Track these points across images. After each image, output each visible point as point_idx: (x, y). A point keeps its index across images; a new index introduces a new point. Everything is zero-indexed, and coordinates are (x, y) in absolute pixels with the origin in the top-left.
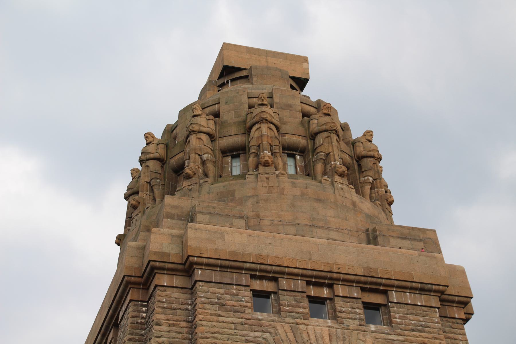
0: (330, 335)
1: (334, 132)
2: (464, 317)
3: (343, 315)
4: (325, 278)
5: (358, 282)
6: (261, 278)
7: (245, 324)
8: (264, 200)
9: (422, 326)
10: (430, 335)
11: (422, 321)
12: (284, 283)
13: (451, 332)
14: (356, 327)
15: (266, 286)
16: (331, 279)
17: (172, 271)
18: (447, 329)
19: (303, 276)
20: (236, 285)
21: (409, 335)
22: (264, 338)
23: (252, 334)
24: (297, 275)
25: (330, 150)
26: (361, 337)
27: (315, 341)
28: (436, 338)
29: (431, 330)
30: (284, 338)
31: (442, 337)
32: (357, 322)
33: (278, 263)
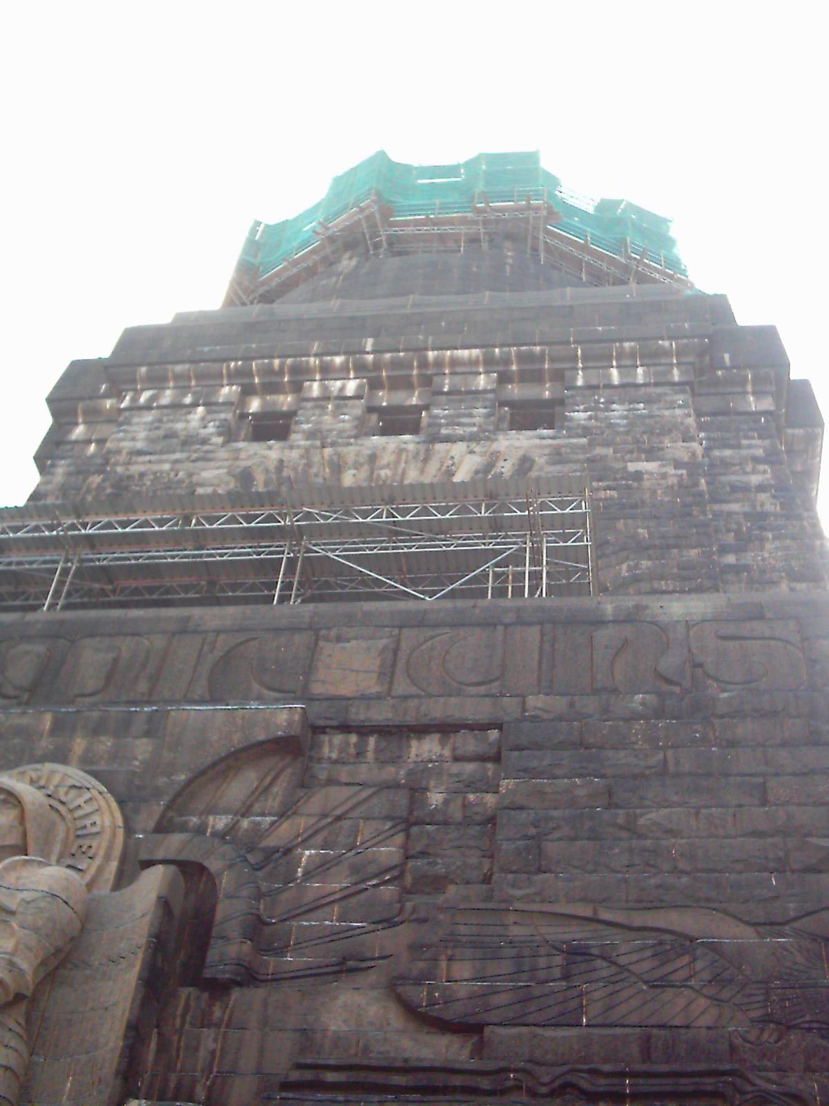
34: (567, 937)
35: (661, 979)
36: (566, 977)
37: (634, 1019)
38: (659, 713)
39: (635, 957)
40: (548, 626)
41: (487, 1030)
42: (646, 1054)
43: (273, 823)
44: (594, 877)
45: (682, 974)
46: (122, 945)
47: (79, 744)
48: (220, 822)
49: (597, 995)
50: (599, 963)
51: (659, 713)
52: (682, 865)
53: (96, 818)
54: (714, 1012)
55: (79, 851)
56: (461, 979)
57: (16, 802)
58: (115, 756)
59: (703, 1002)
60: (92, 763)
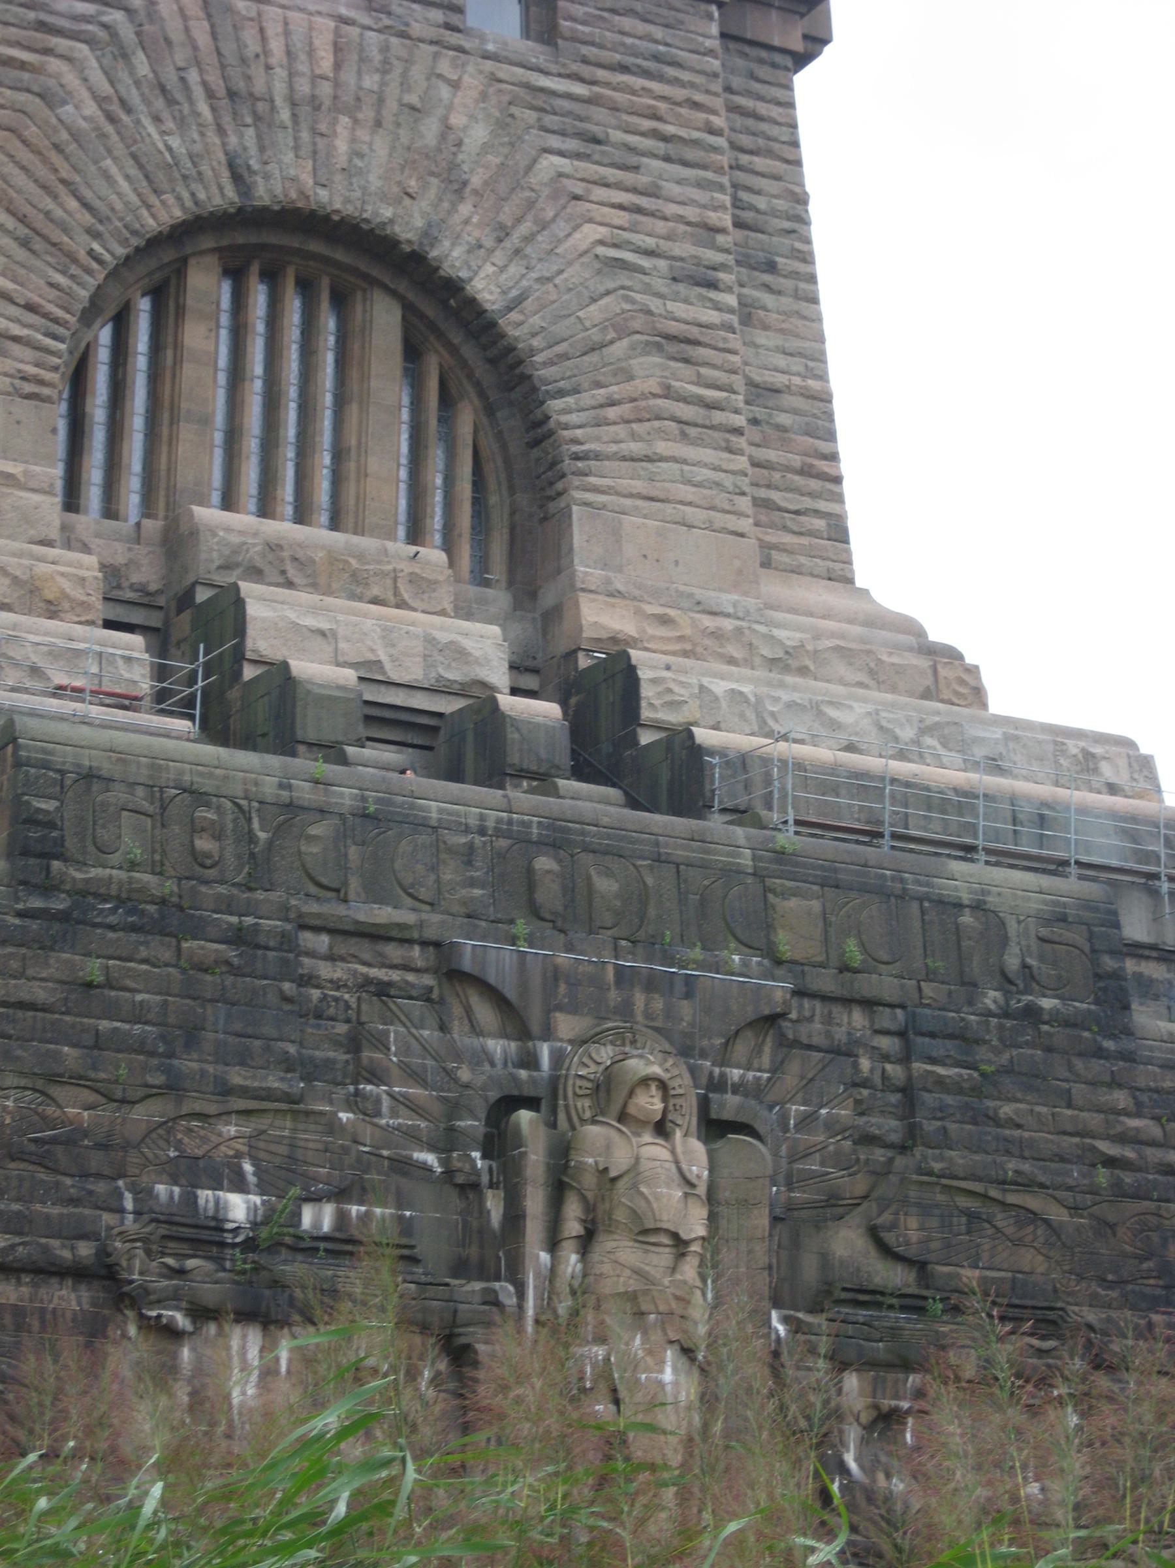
0: (337, 49)
2: (798, 46)
9: (656, 58)
10: (680, 94)
11: (657, 42)
13: (749, 94)
14: (432, 33)
18: (737, 82)
21: (607, 85)
22: (105, 26)
26: (444, 67)
27: (285, 61)
28: (696, 105)
29: (685, 76)
30: (176, 36)
31: (718, 103)
34: (969, 1205)
35: (1020, 1239)
36: (968, 1233)
37: (1005, 1266)
38: (1006, 1014)
39: (1005, 1223)
40: (926, 904)
41: (930, 1267)
42: (1013, 1289)
43: (769, 1079)
44: (977, 1157)
45: (1031, 1237)
47: (639, 999)
48: (735, 1074)
49: (986, 1247)
50: (986, 1225)
51: (1006, 1014)
52: (1027, 1153)
54: (1046, 1265)
56: (911, 1231)
58: (669, 1013)
59: (1041, 1258)
60: (653, 1019)
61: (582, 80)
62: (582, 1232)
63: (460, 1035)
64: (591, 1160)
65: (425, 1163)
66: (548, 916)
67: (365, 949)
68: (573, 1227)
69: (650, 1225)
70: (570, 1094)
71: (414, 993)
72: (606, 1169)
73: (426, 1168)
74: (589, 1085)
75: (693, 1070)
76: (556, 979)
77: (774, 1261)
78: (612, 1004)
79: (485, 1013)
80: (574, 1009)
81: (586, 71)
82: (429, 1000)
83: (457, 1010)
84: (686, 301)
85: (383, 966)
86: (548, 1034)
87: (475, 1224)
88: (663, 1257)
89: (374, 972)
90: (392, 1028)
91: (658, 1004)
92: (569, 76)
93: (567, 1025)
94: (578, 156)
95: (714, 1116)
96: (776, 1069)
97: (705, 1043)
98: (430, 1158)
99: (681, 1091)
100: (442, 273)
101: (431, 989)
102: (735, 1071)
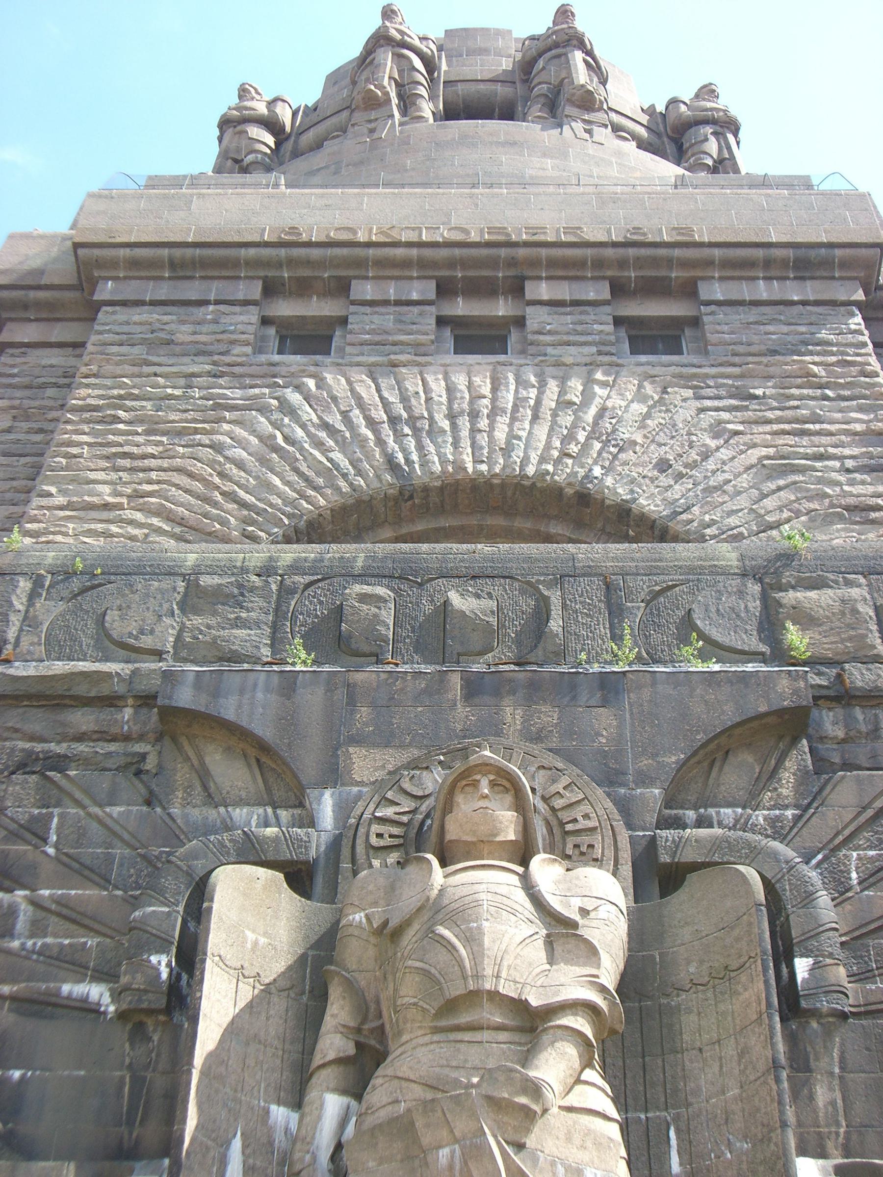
1: (575, 42)
3: (548, 338)
4: (494, 263)
5: (599, 264)
6: (303, 288)
7: (222, 375)
8: (355, 165)
11: (802, 333)
12: (366, 290)
15: (318, 308)
16: (512, 263)
17: (49, 312)
19: (423, 264)
20: (217, 302)
23: (238, 393)
24: (406, 264)
25: (563, 75)
32: (594, 349)
33: (344, 236)
43: (797, 819)
46: (692, 969)
53: (585, 808)
55: (577, 852)
57: (508, 785)
61: (734, 365)
62: (351, 1050)
63: (183, 810)
64: (359, 917)
65: (85, 999)
66: (366, 648)
67: (37, 721)
68: (333, 1043)
69: (455, 990)
70: (360, 849)
71: (110, 764)
72: (386, 923)
73: (87, 1010)
74: (396, 831)
75: (625, 808)
76: (352, 702)
77: (838, 1095)
78: (459, 727)
79: (230, 773)
80: (384, 738)
81: (737, 360)
82: (138, 773)
83: (182, 774)
84: (863, 483)
85: (64, 738)
86: (334, 775)
87: (160, 1083)
88: (496, 1049)
89: (39, 747)
90: (56, 811)
91: (548, 715)
92: (721, 365)
93: (366, 764)
94: (736, 408)
95: (665, 858)
96: (810, 800)
97: (645, 762)
98: (97, 992)
99: (583, 824)
100: (608, 502)
101: (143, 757)
102: (729, 811)
